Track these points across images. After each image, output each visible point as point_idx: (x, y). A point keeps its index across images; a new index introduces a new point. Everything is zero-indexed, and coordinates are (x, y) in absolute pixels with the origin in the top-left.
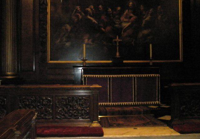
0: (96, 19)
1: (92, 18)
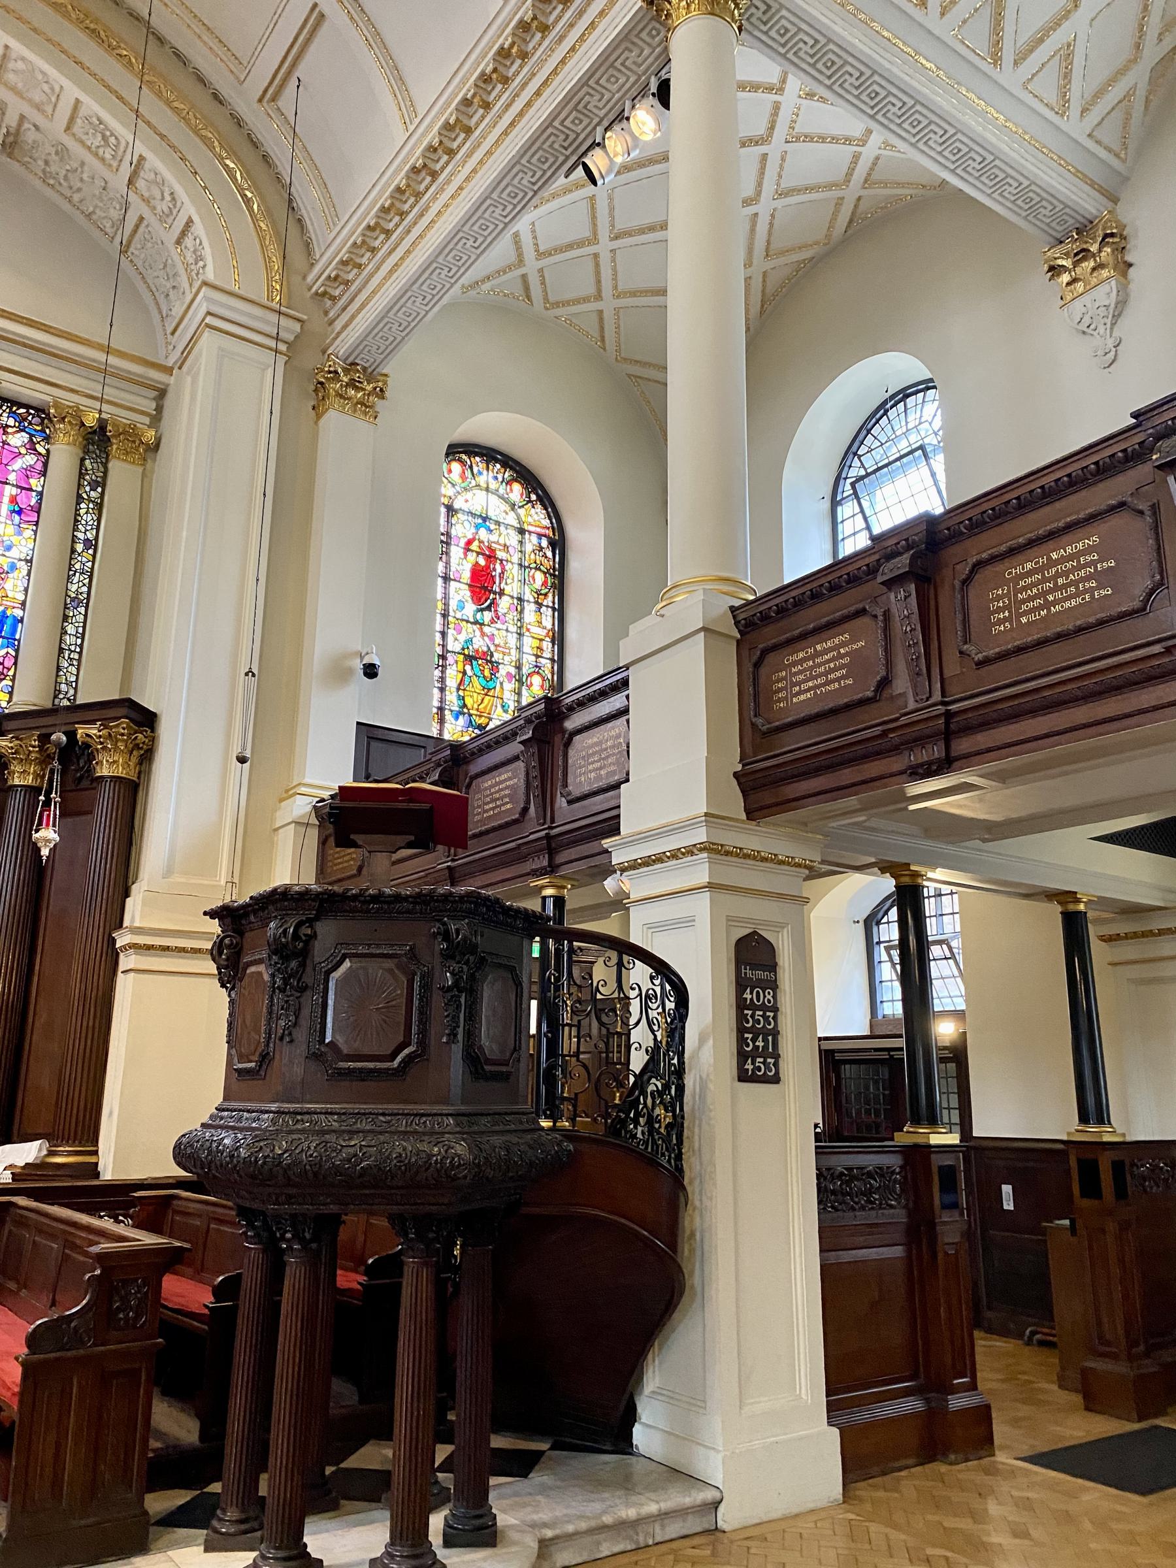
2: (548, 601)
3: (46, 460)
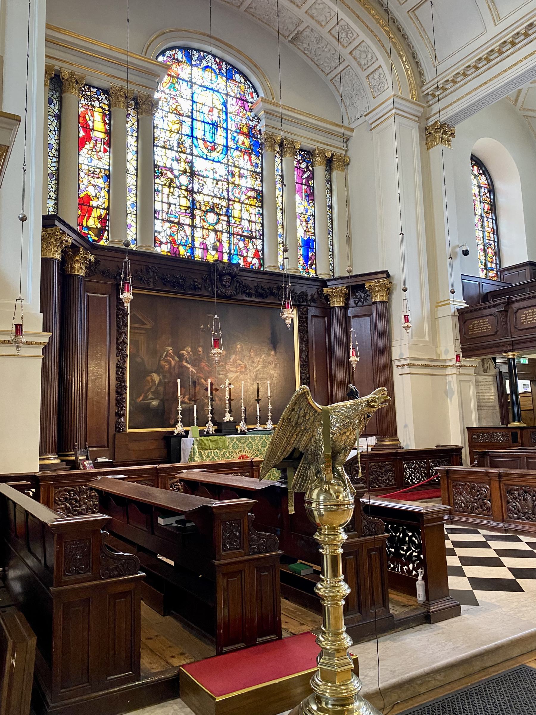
0: (193, 366)
1: (188, 366)
2: (490, 216)
3: (312, 172)
